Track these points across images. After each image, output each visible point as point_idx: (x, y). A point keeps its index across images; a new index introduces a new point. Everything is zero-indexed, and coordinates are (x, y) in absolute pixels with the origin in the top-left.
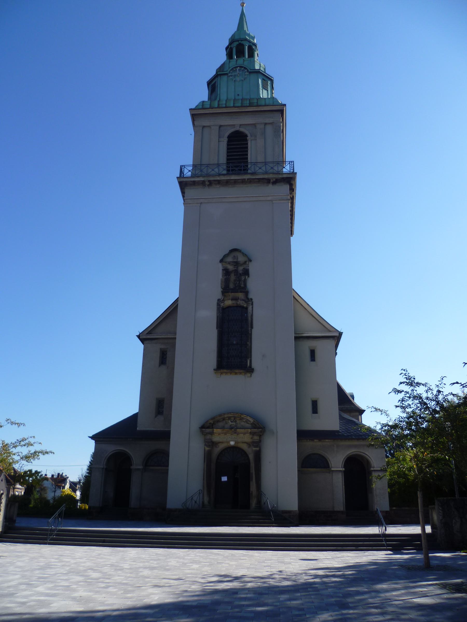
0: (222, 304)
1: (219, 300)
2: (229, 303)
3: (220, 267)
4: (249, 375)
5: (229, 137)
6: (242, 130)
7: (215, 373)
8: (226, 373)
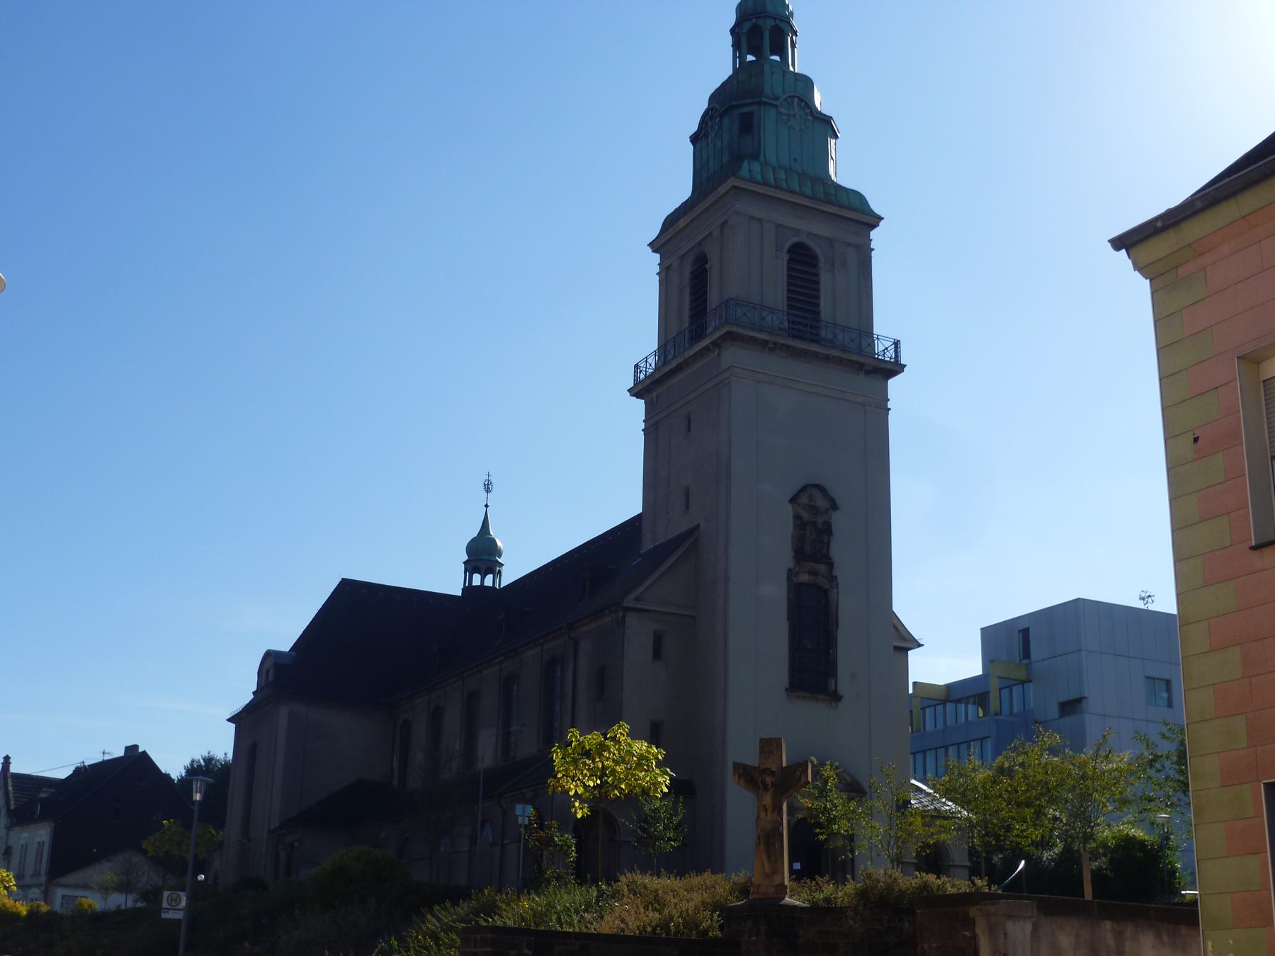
0: (795, 579)
1: (790, 570)
2: (804, 578)
3: (788, 512)
4: (834, 704)
5: (789, 251)
6: (811, 243)
7: (788, 696)
8: (804, 697)
